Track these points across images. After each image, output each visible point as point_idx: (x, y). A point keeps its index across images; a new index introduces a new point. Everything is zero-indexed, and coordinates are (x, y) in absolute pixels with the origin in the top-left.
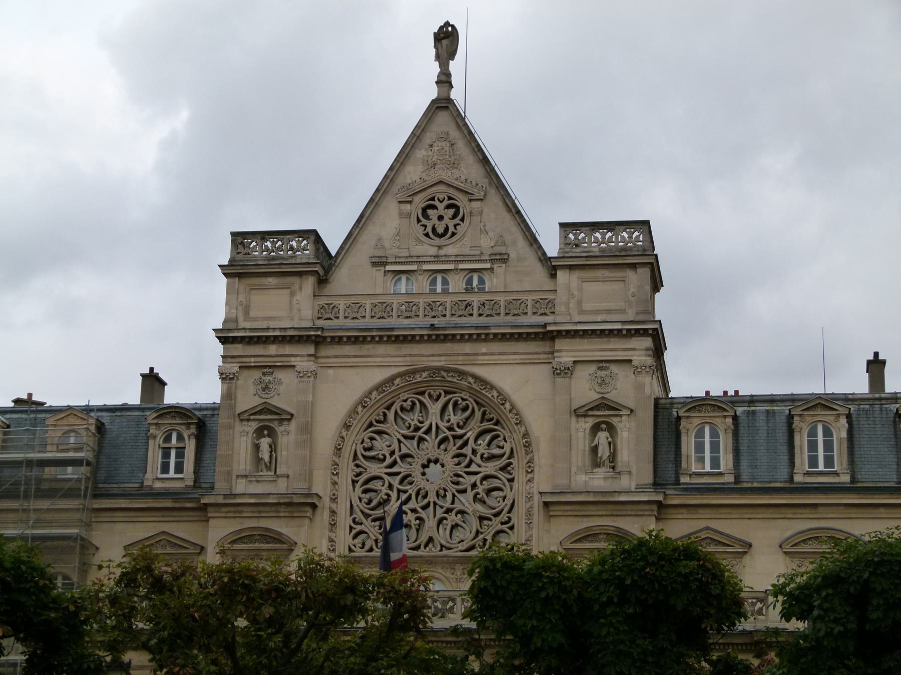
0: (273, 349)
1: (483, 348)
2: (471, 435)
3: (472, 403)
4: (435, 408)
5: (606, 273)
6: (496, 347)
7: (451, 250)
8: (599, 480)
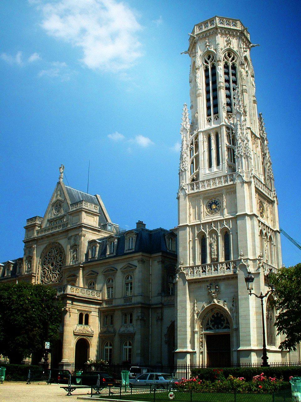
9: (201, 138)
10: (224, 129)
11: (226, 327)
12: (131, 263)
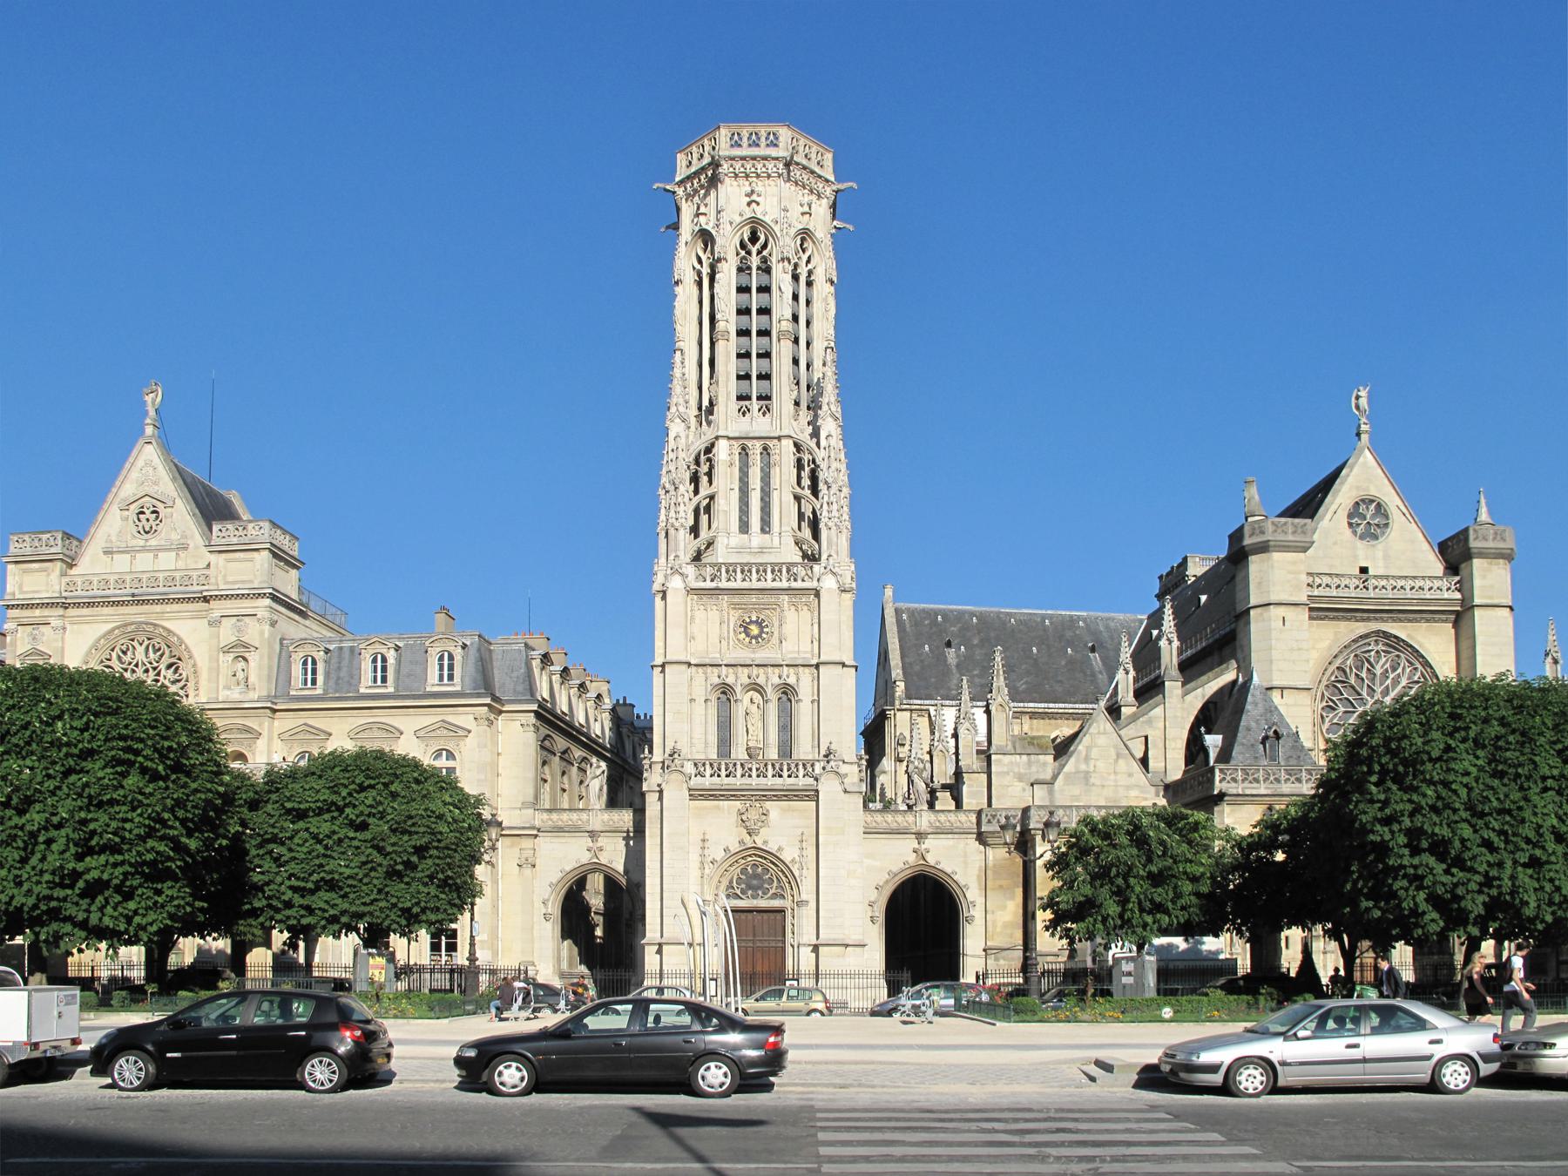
0: (37, 612)
1: (168, 608)
2: (162, 667)
3: (164, 646)
4: (140, 650)
5: (241, 555)
6: (175, 607)
7: (153, 542)
8: (235, 694)
9: (723, 451)
10: (788, 445)
11: (775, 896)
12: (450, 719)
